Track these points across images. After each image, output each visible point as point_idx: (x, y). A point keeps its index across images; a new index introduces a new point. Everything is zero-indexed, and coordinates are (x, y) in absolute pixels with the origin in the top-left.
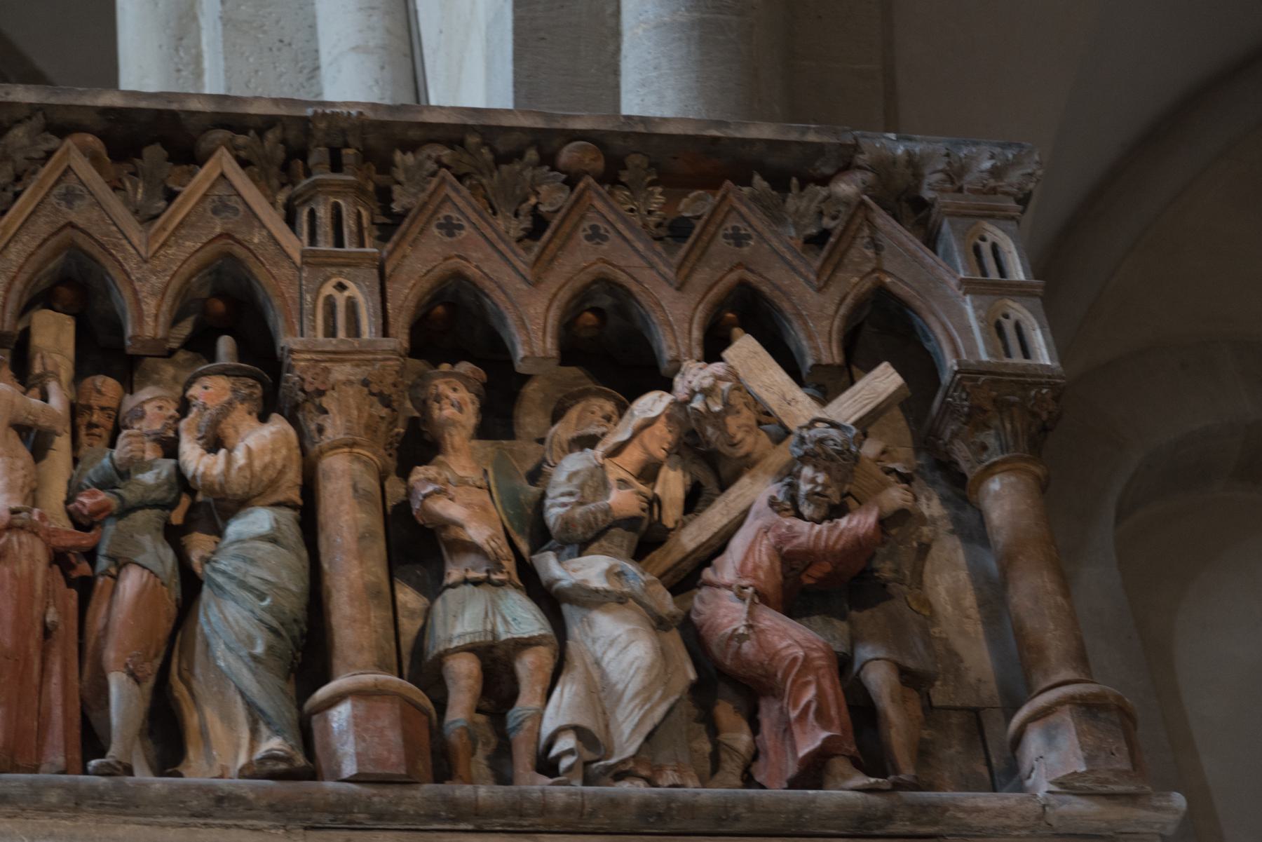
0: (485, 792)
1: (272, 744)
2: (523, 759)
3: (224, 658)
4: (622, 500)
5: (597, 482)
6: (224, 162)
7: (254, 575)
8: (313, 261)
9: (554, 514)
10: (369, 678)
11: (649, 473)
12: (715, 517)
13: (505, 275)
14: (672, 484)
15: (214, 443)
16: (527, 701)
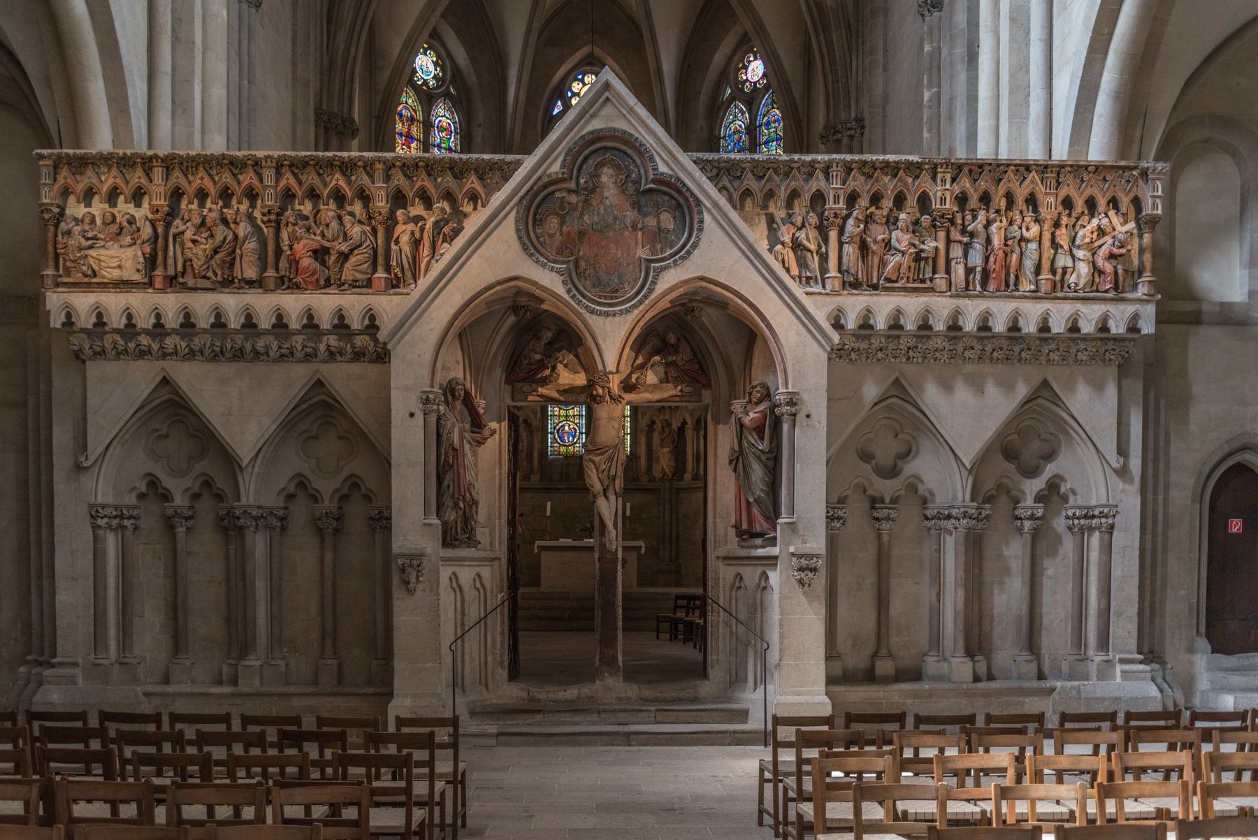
0: (1060, 294)
1: (1033, 287)
2: (1066, 286)
3: (1028, 273)
4: (1087, 240)
5: (1084, 236)
6: (1034, 173)
7: (1033, 257)
8: (1047, 194)
9: (1077, 243)
10: (1047, 277)
11: (1092, 232)
12: (1101, 242)
13: (1076, 195)
14: (1095, 234)
15: (1028, 229)
16: (1067, 276)
